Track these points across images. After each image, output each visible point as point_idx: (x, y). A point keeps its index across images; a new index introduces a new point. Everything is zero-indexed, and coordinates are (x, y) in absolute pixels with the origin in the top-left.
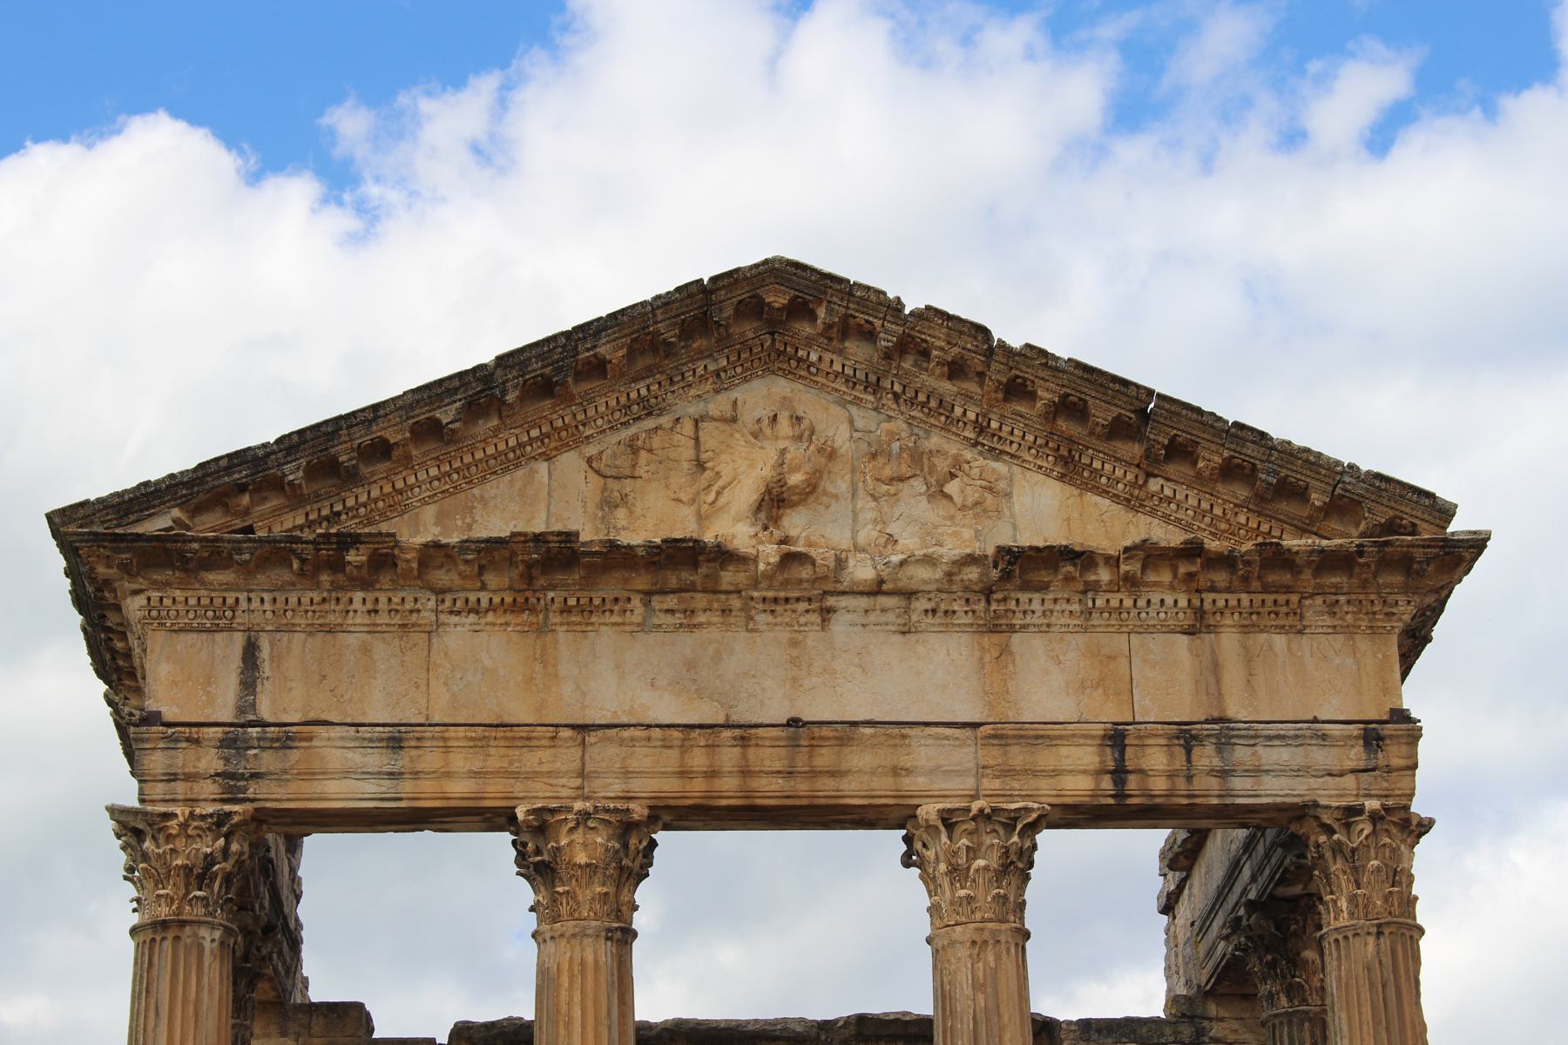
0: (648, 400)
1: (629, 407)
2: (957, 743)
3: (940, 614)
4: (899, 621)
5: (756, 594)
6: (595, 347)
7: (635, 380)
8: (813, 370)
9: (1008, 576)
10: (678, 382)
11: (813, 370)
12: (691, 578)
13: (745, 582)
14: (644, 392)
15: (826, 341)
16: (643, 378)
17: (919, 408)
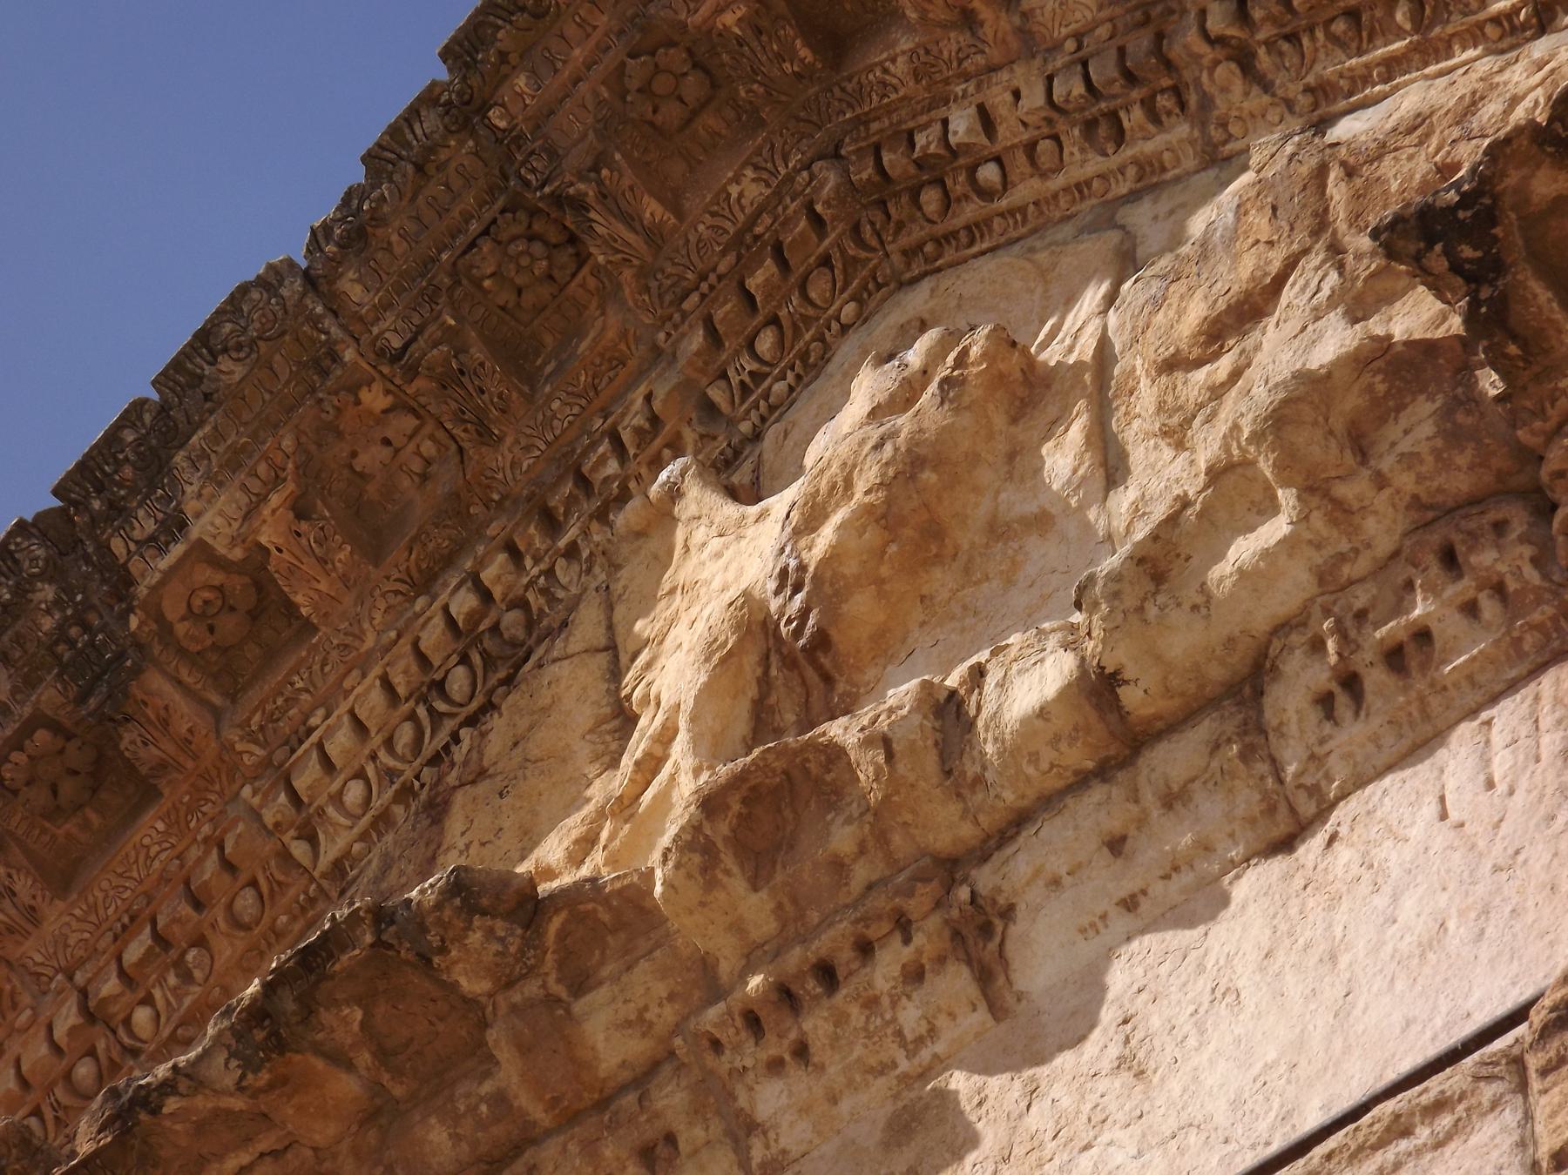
0: (495, 629)
1: (440, 686)
2: (1445, 1121)
3: (1375, 678)
4: (1247, 799)
5: (713, 1013)
6: (175, 525)
7: (424, 582)
8: (989, 173)
9: (1514, 338)
10: (571, 501)
11: (989, 173)
12: (487, 1088)
13: (661, 989)
14: (463, 603)
15: (964, 38)
16: (448, 561)
17: (1320, 34)
